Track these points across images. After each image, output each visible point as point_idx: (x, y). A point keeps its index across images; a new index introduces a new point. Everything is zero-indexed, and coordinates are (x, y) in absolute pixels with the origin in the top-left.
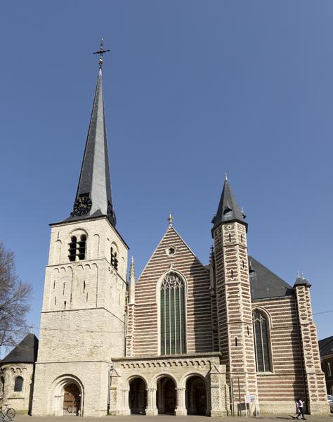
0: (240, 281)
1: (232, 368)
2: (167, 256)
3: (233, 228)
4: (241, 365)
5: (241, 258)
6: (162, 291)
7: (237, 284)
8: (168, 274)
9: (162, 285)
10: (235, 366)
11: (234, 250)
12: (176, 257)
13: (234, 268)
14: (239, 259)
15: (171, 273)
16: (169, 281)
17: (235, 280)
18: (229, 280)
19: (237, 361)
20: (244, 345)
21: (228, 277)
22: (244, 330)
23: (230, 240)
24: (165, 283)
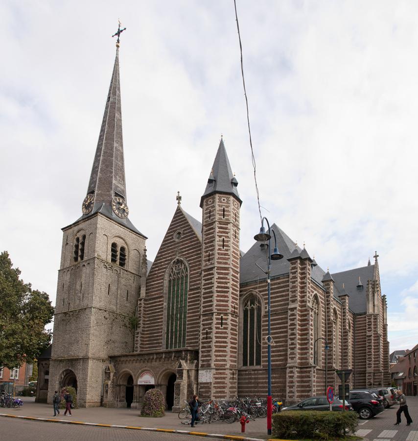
0: (216, 265)
1: (200, 363)
2: (174, 241)
3: (213, 202)
4: (209, 361)
5: (220, 237)
6: (170, 281)
7: (212, 269)
8: (174, 262)
9: (170, 275)
10: (203, 361)
11: (212, 229)
12: (182, 242)
13: (212, 250)
14: (217, 239)
15: (178, 260)
16: (176, 269)
17: (211, 264)
18: (206, 265)
19: (206, 356)
20: (214, 338)
21: (205, 261)
22: (215, 321)
23: (210, 217)
24: (172, 272)
